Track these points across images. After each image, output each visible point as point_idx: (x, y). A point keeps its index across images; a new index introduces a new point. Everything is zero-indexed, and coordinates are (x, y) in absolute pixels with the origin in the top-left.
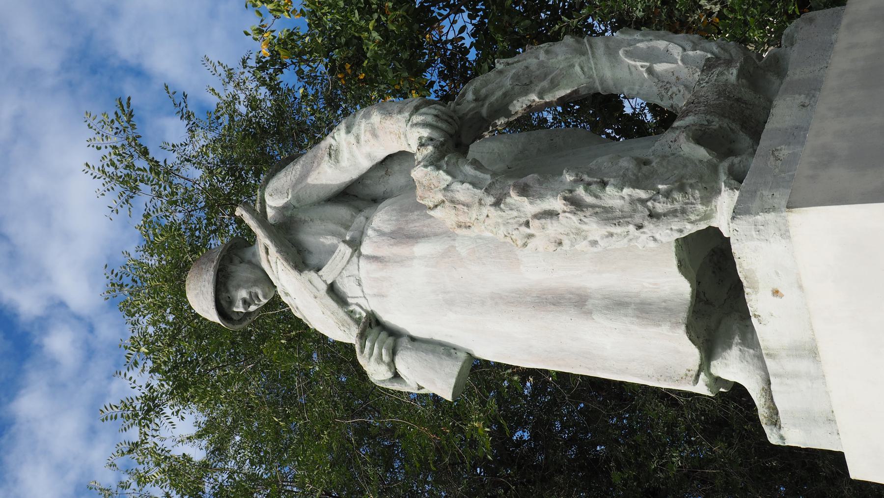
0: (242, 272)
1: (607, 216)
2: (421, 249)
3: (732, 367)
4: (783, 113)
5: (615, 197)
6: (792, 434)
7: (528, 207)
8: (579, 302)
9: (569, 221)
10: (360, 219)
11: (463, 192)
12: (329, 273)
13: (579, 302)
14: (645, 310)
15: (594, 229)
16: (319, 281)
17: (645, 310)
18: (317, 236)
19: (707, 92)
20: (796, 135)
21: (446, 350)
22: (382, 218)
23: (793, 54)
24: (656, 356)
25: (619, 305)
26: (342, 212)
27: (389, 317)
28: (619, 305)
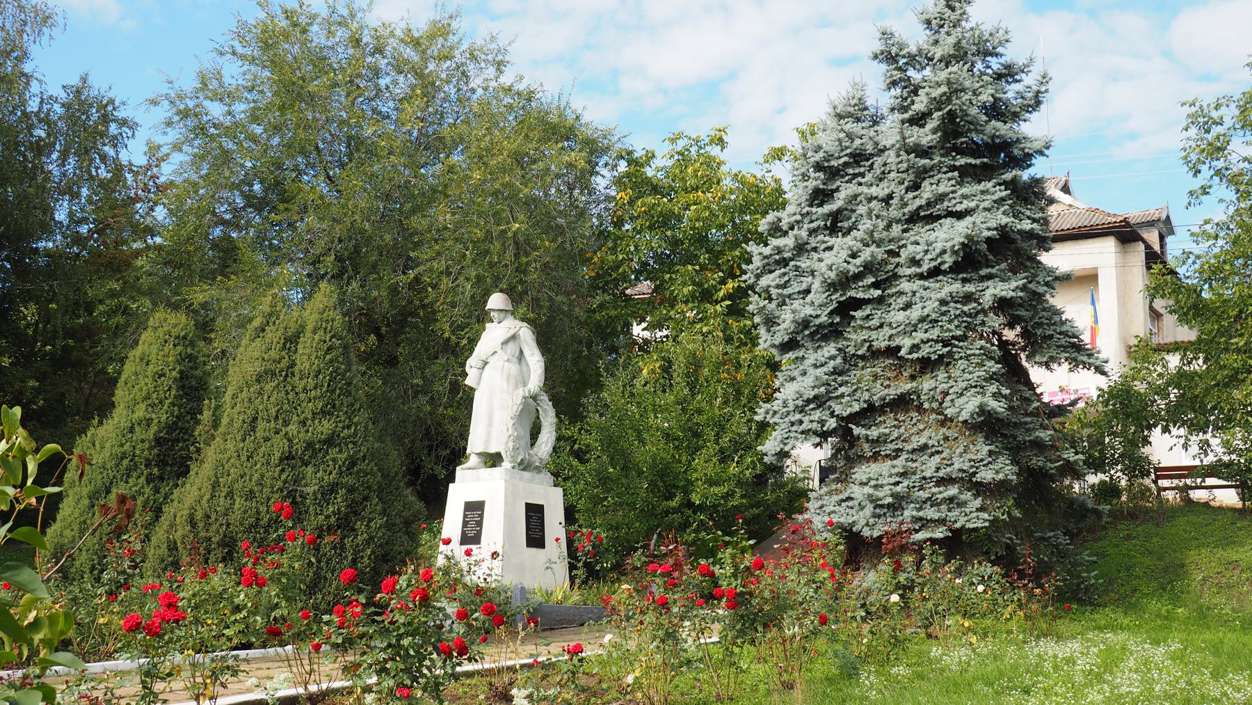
0: (502, 315)
1: (507, 443)
2: (505, 383)
3: (473, 460)
4: (527, 475)
5: (511, 445)
6: (459, 471)
7: (510, 425)
8: (490, 425)
9: (507, 434)
10: (515, 360)
11: (515, 408)
12: (500, 352)
13: (490, 425)
14: (487, 442)
15: (505, 440)
16: (498, 349)
17: (487, 442)
18: (511, 347)
19: (535, 458)
20: (522, 479)
21: (478, 384)
22: (513, 368)
23: (542, 475)
24: (477, 442)
25: (489, 434)
26: (517, 354)
27: (487, 367)
28: (489, 434)
